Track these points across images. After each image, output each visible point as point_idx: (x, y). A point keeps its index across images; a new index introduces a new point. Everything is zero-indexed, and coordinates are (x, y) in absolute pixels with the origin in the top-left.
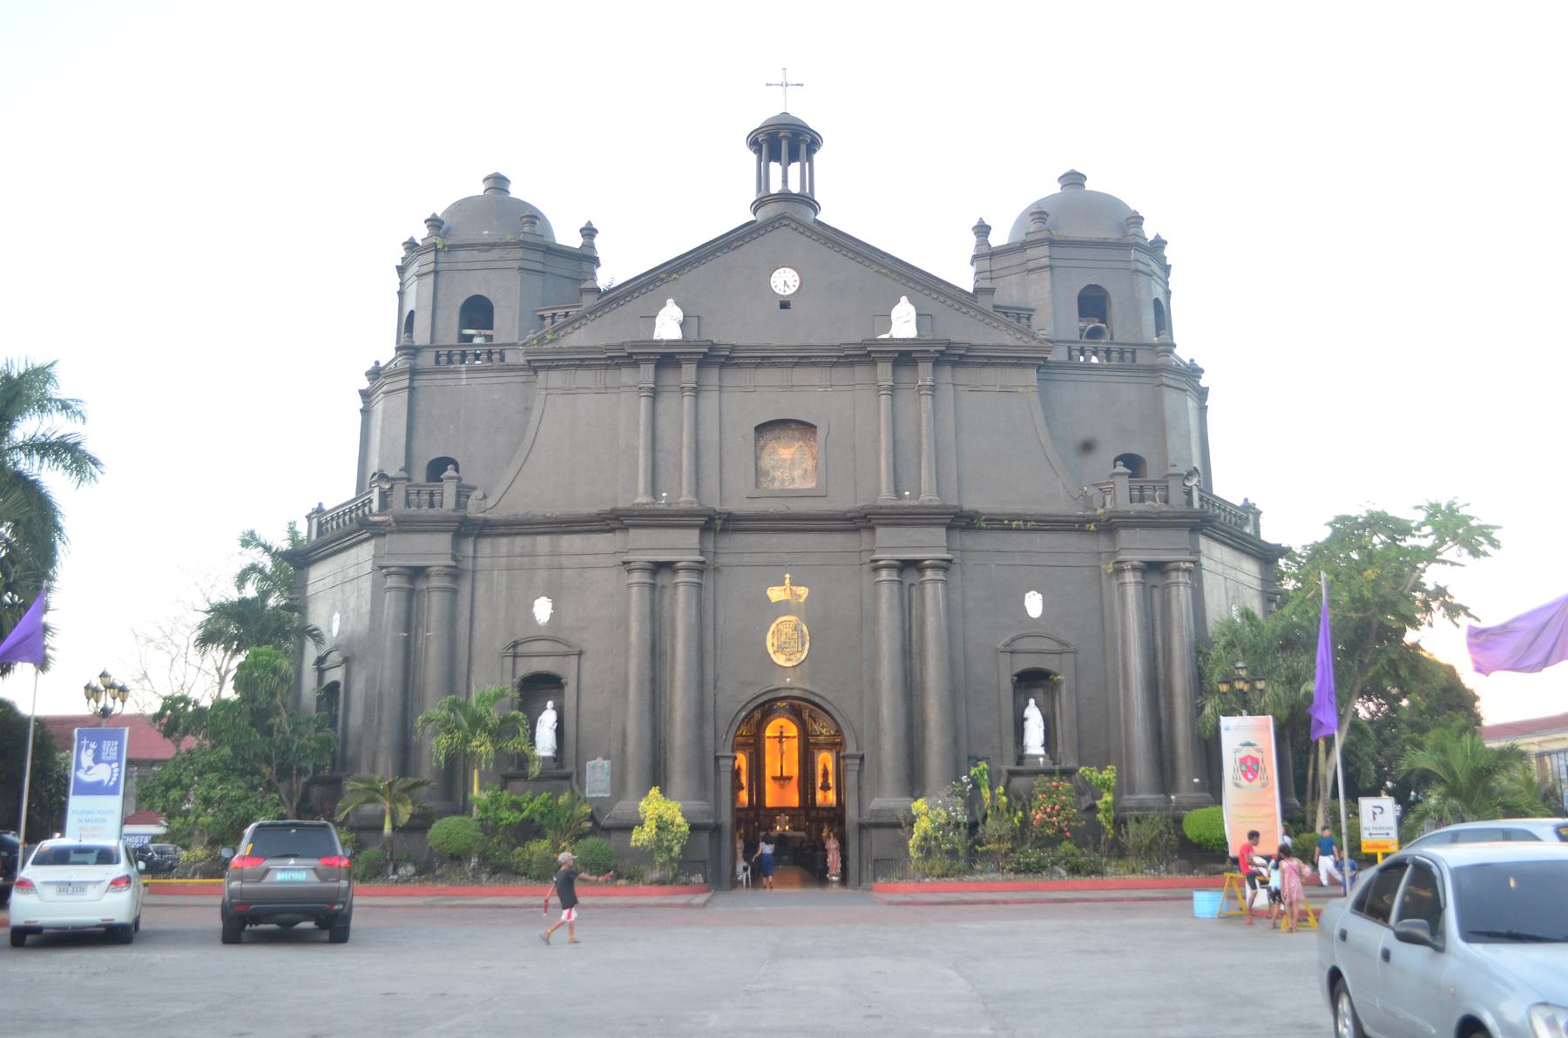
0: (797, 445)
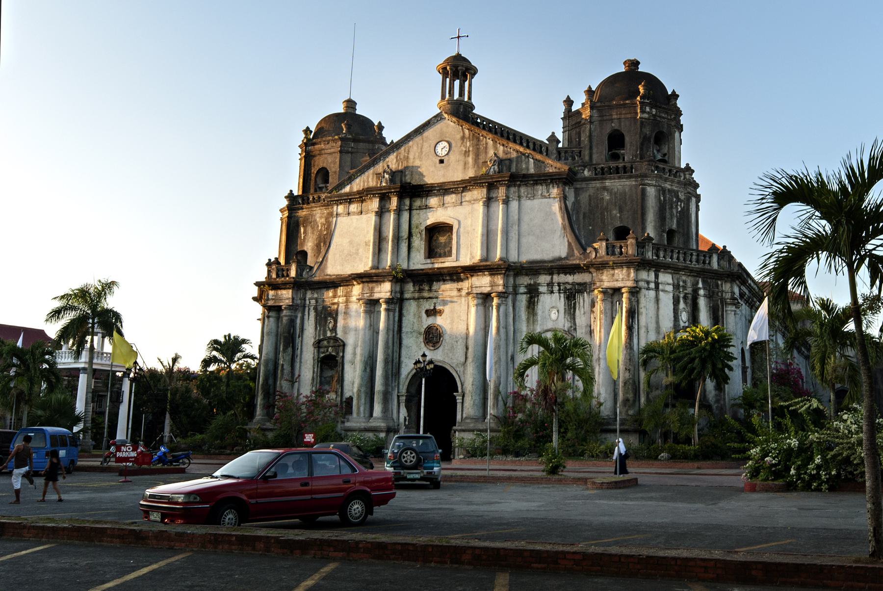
0: (448, 235)
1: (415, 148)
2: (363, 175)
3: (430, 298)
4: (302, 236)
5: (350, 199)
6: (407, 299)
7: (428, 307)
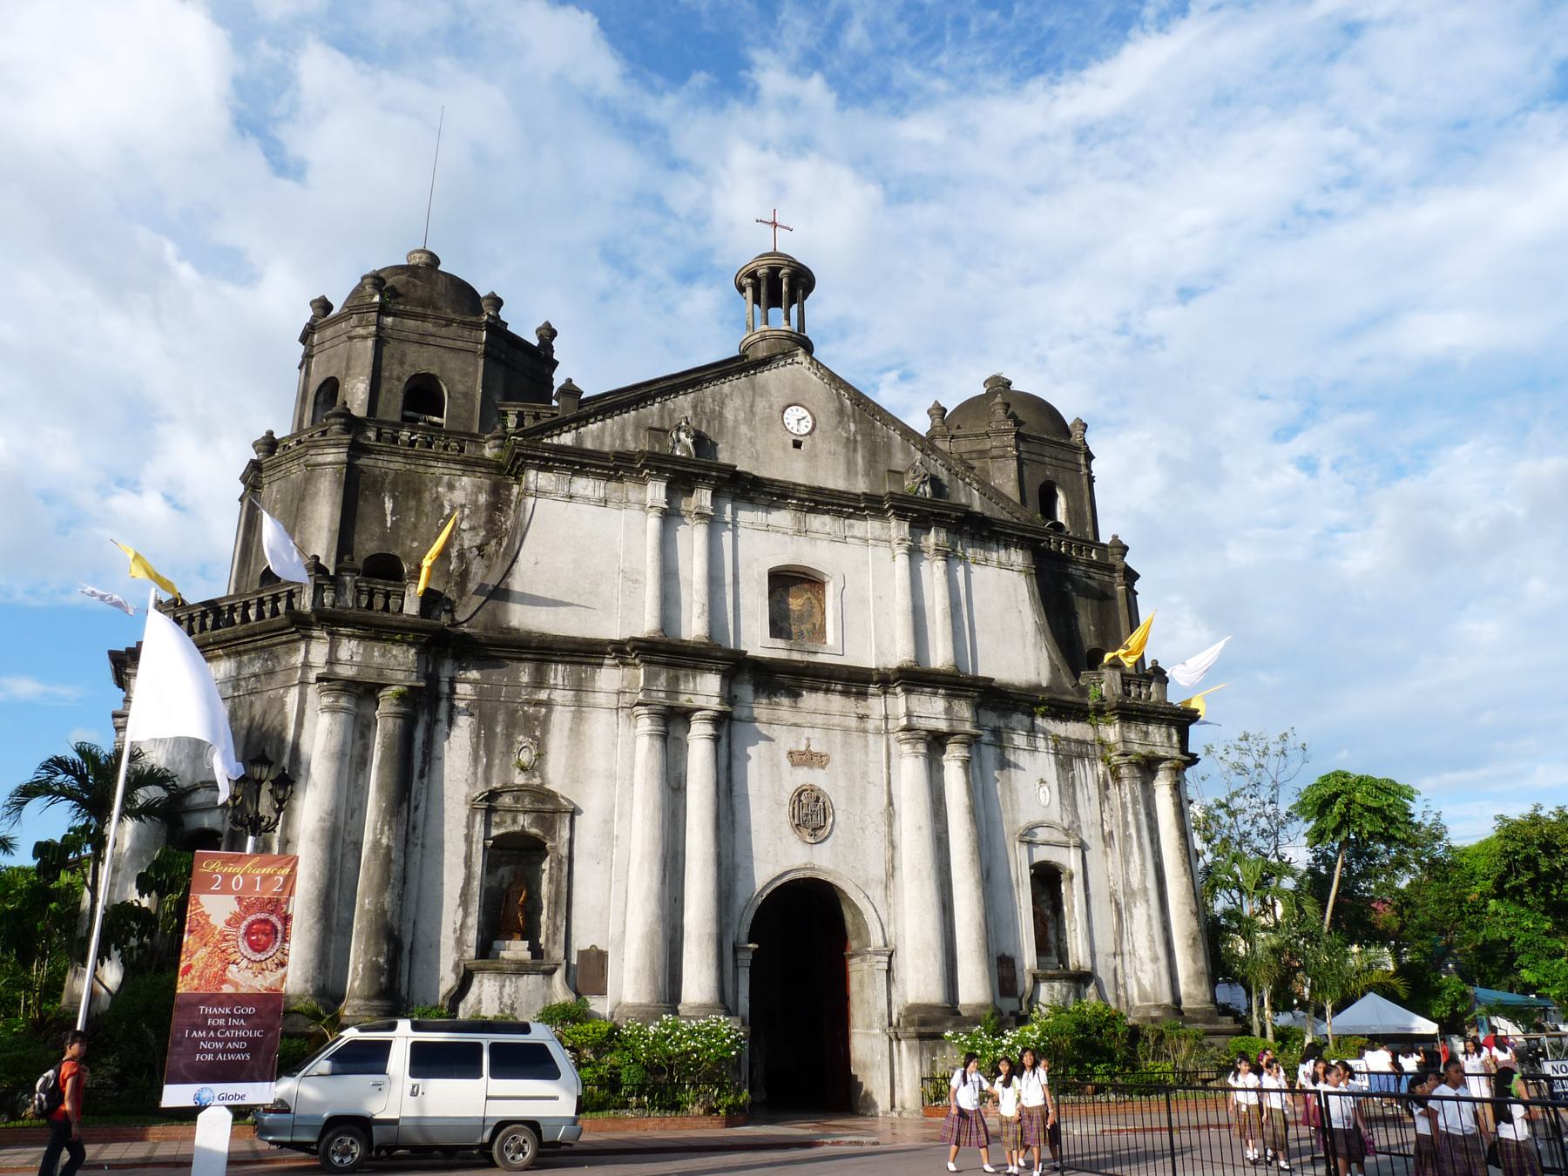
0: (806, 597)
1: (738, 402)
2: (609, 421)
3: (796, 725)
4: (389, 518)
5: (583, 465)
6: (740, 720)
7: (794, 749)
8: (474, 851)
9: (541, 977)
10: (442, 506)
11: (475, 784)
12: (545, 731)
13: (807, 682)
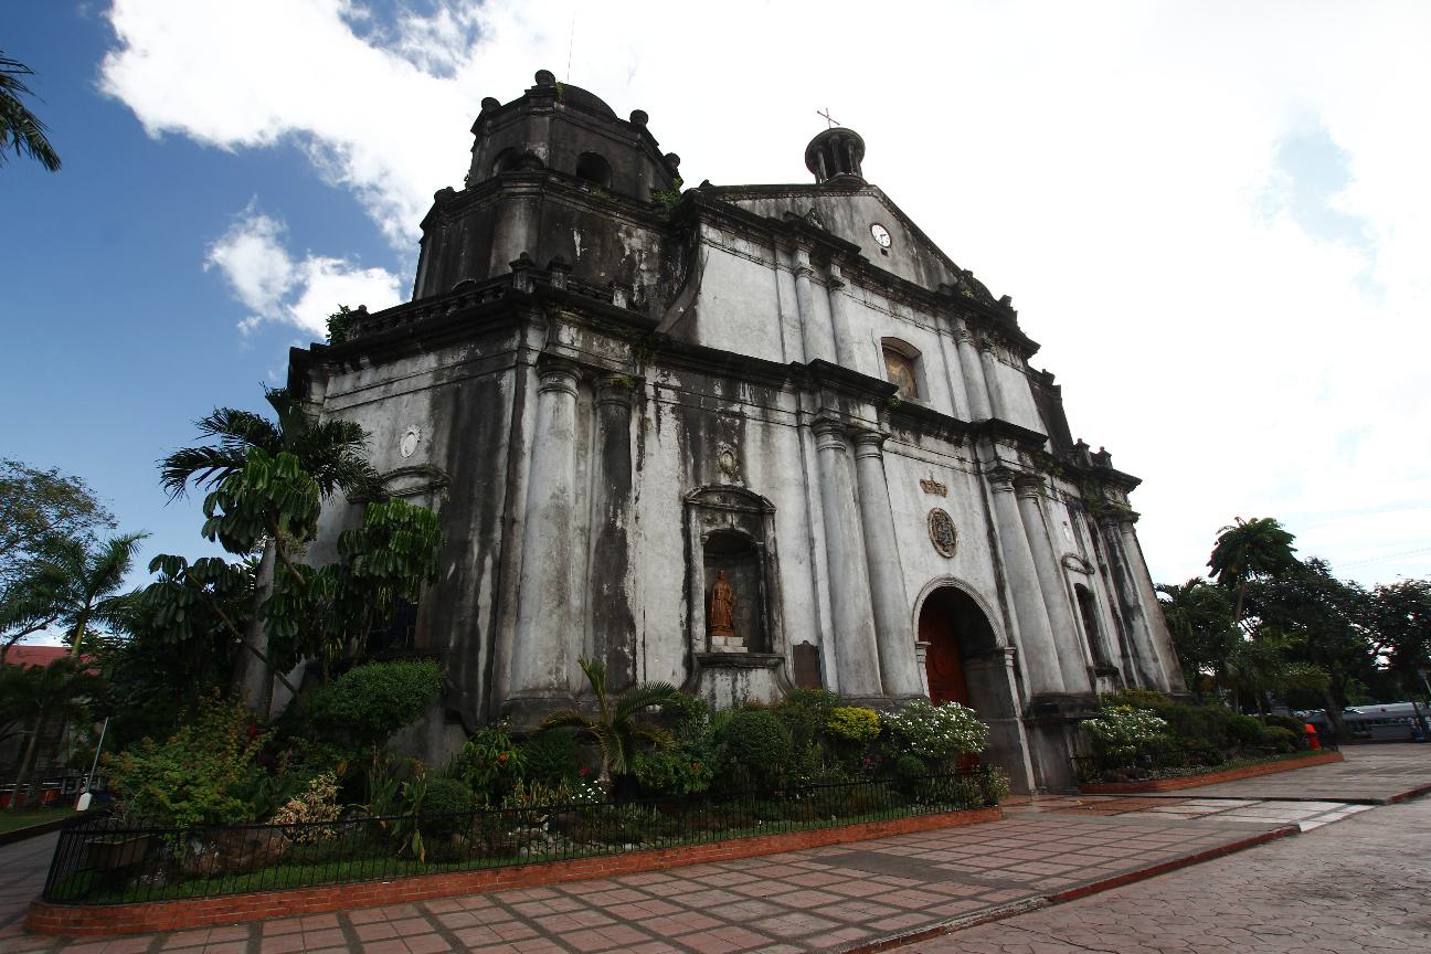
4: (578, 249)
5: (746, 226)
8: (693, 544)
9: (766, 671)
10: (623, 249)
11: (686, 482)
12: (742, 440)
13: (925, 426)
